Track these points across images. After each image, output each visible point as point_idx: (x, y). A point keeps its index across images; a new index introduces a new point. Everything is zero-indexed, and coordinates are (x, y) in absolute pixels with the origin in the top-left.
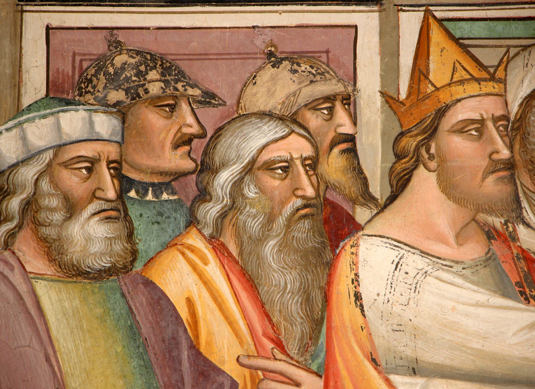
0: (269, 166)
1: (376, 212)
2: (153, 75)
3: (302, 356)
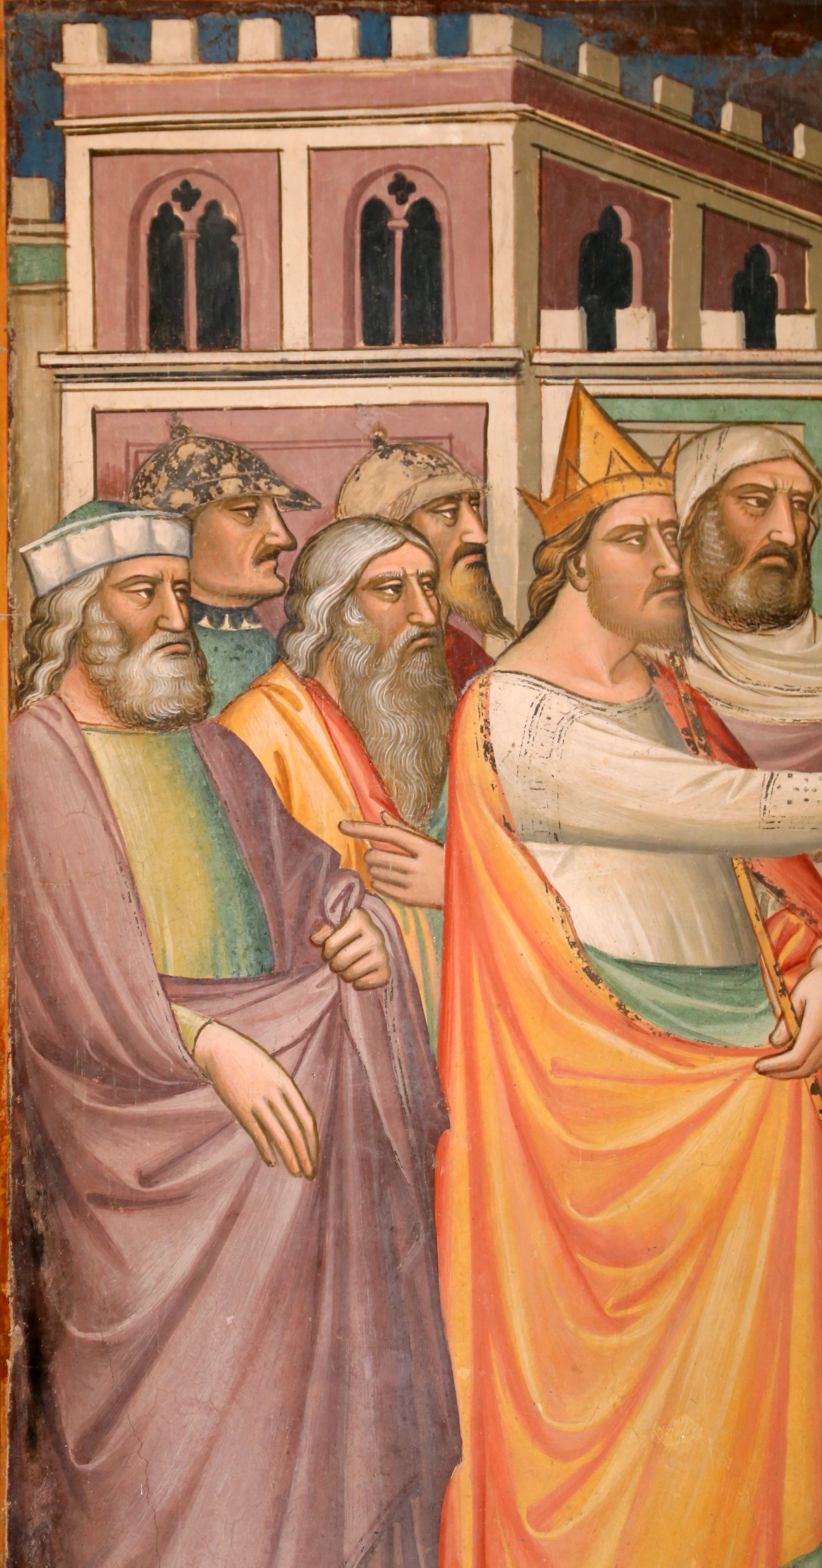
0: (376, 586)
1: (510, 642)
2: (228, 469)
3: (419, 820)
